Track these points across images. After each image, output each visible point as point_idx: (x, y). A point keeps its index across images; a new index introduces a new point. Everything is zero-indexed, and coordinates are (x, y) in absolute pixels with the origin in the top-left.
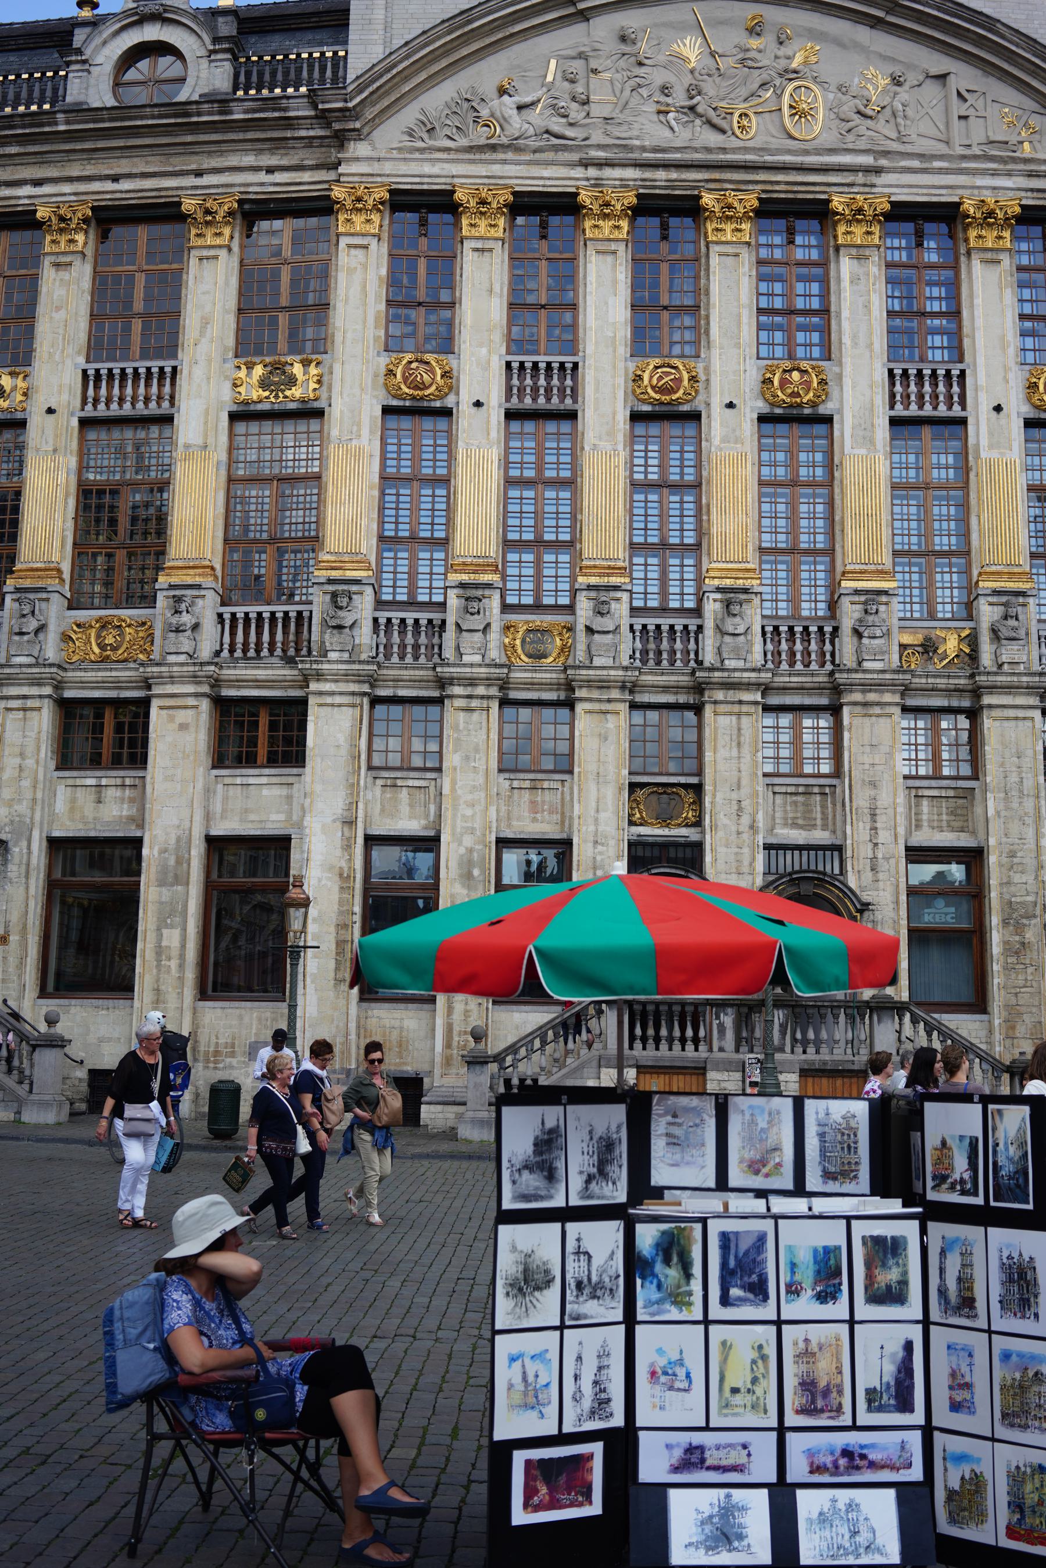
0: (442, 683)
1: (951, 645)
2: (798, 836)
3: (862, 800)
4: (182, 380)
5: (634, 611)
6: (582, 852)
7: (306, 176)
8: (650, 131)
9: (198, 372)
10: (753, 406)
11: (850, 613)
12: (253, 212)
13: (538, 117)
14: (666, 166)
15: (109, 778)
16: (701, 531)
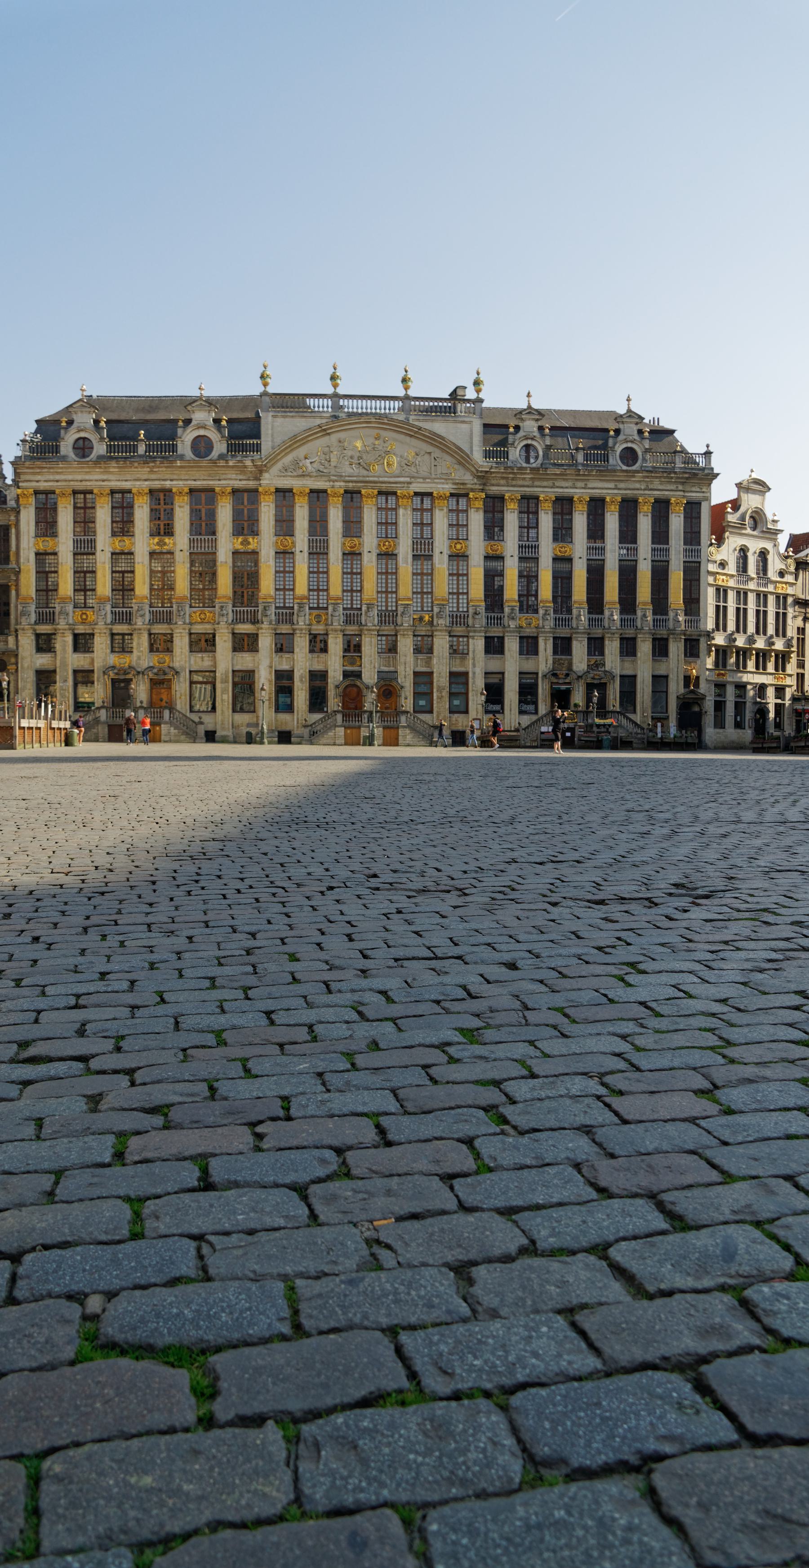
0: (294, 630)
1: (427, 618)
2: (386, 669)
3: (402, 659)
4: (219, 543)
5: (344, 609)
6: (331, 674)
7: (251, 483)
8: (347, 470)
9: (223, 540)
10: (375, 552)
11: (400, 609)
12: (235, 491)
13: (315, 465)
14: (352, 482)
15: (205, 655)
16: (361, 586)
